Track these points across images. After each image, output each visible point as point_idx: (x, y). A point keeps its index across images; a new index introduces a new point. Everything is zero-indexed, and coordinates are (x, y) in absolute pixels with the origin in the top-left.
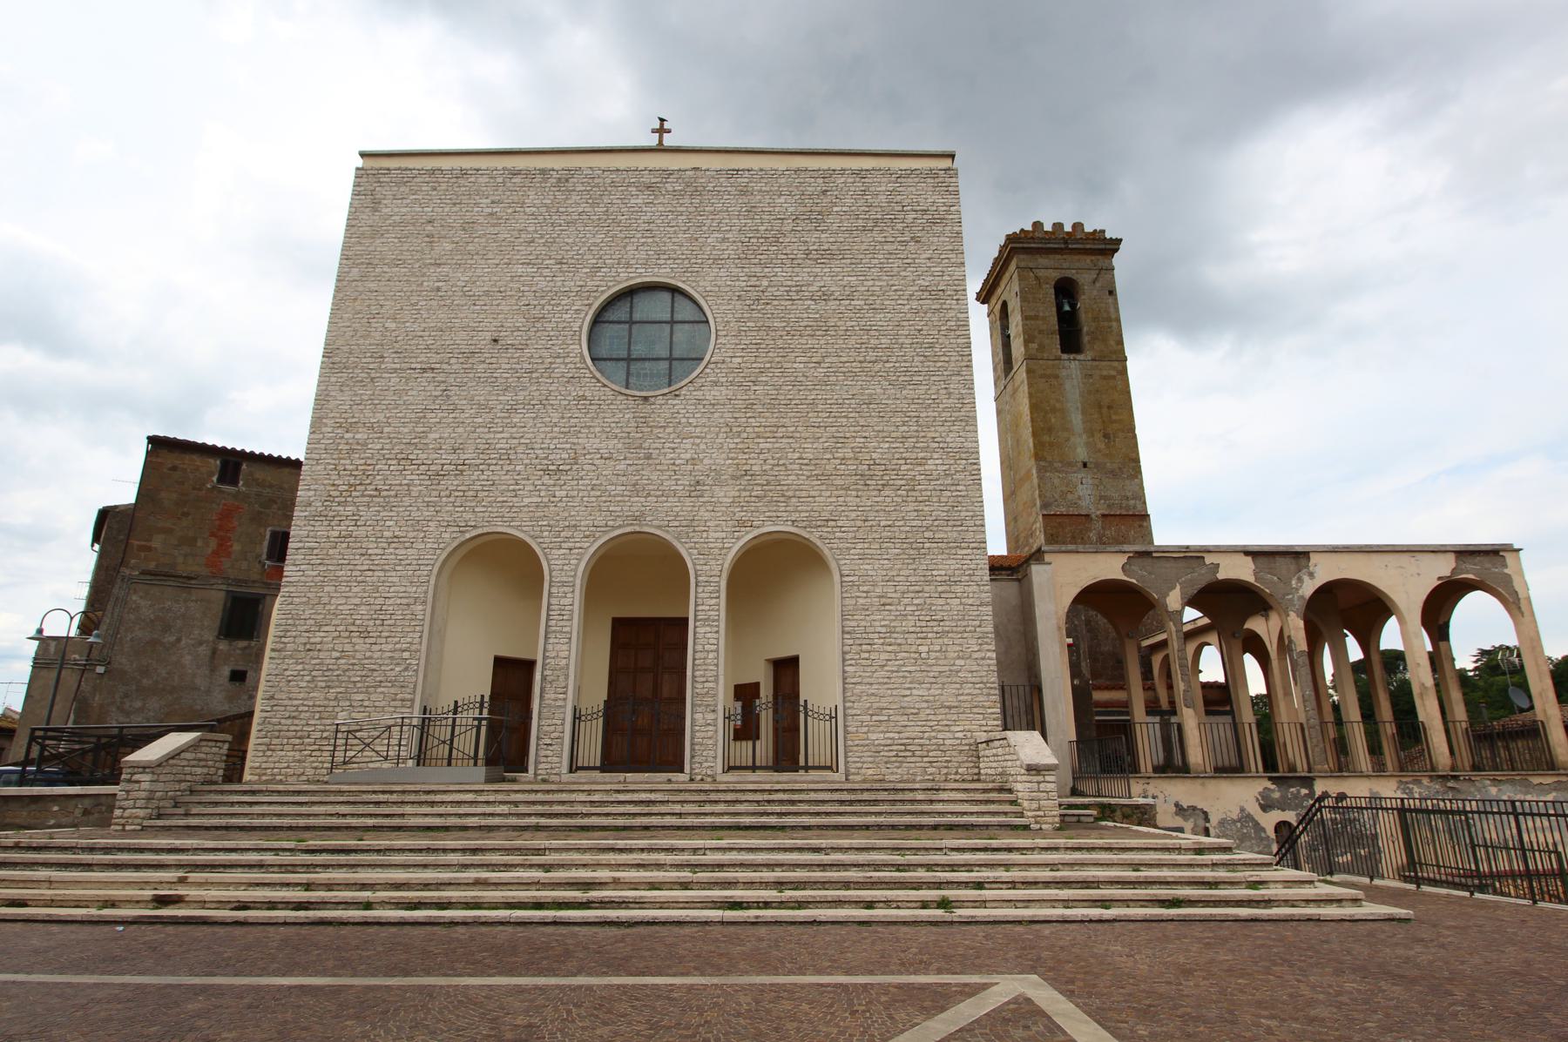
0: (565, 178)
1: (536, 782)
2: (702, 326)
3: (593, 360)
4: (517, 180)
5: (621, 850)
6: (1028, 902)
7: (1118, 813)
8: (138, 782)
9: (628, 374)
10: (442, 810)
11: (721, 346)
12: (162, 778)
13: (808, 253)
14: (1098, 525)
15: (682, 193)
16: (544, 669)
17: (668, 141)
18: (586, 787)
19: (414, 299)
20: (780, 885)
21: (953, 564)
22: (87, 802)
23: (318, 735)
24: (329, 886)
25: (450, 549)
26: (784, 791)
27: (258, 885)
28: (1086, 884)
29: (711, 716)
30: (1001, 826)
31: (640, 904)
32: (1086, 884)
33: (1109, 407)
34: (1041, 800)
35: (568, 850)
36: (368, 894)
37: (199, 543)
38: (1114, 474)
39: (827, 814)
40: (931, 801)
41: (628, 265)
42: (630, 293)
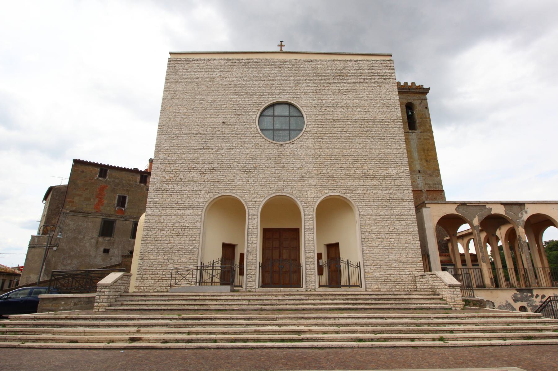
0: (248, 61)
1: (246, 292)
2: (300, 118)
3: (261, 130)
4: (229, 63)
5: (306, 318)
6: (474, 338)
7: (471, 303)
8: (104, 292)
9: (274, 135)
10: (221, 302)
11: (309, 124)
12: (112, 290)
13: (339, 91)
14: (425, 194)
15: (291, 68)
16: (247, 248)
17: (284, 49)
18: (274, 294)
19: (192, 107)
20: (374, 332)
21: (401, 208)
22: (76, 300)
23: (161, 273)
24: (197, 333)
25: (209, 201)
26: (351, 295)
27: (168, 333)
28: (492, 331)
29: (313, 266)
30: (441, 308)
31: (322, 340)
32: (492, 331)
33: (427, 150)
34: (454, 298)
35: (285, 318)
36: (214, 336)
37: (92, 200)
38: (430, 175)
39: (372, 304)
40: (410, 299)
41: (272, 95)
42: (273, 105)
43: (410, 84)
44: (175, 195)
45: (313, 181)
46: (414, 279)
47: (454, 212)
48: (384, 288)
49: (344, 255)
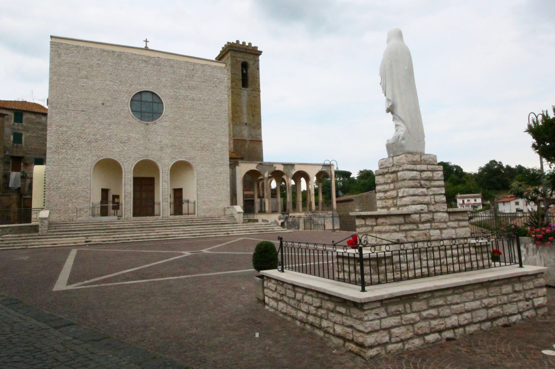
3: (132, 111)
4: (105, 53)
9: (141, 116)
13: (189, 87)
22: (10, 229)
29: (167, 204)
42: (141, 93)
43: (247, 44)
44: (68, 157)
45: (169, 151)
46: (225, 210)
47: (255, 169)
48: (208, 215)
49: (185, 197)
